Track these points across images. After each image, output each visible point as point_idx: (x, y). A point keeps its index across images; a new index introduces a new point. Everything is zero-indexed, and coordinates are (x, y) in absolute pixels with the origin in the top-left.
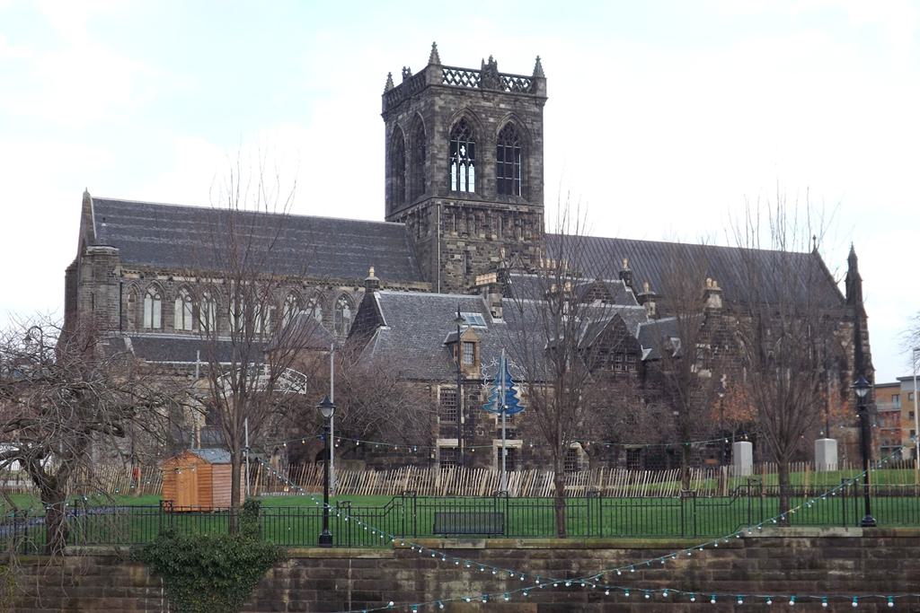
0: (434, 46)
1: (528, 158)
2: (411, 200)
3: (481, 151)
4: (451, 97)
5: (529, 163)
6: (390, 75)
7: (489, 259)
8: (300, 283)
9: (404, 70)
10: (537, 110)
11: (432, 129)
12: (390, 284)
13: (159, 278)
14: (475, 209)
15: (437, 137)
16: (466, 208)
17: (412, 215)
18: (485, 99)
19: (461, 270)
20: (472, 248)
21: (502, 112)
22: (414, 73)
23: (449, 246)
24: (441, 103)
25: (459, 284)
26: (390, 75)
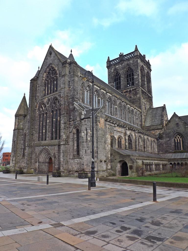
0: (136, 46)
2: (125, 88)
4: (140, 61)
6: (109, 57)
8: (121, 100)
9: (121, 53)
10: (150, 72)
13: (90, 83)
14: (145, 93)
15: (139, 70)
17: (127, 92)
18: (144, 65)
19: (145, 109)
20: (145, 103)
22: (124, 55)
23: (143, 101)
26: (109, 57)
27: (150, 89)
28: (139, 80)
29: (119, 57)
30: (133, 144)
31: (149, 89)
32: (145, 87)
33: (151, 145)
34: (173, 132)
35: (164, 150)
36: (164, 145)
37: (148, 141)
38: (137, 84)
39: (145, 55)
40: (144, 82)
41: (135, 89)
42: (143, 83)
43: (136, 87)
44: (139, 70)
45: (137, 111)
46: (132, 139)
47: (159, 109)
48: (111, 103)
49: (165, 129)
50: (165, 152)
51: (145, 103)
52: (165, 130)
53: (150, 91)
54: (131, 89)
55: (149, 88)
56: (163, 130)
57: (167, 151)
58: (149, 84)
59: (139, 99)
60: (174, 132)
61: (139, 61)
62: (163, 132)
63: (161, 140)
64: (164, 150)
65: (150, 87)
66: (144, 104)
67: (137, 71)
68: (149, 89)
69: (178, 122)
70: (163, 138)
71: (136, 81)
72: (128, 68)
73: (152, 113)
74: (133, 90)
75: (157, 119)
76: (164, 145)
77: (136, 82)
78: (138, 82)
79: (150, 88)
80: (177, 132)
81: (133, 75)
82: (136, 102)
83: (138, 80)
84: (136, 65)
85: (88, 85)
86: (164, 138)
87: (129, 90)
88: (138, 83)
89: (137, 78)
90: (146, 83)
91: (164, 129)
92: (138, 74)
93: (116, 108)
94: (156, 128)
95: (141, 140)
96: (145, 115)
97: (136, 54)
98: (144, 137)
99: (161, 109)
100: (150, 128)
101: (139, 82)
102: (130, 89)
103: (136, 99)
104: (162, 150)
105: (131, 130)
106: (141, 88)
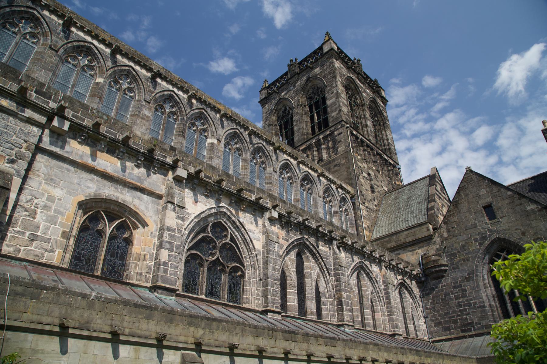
1: (385, 131)
3: (363, 110)
4: (342, 66)
5: (386, 134)
7: (382, 187)
11: (335, 77)
12: (326, 173)
13: (46, 13)
14: (368, 146)
16: (362, 142)
19: (369, 189)
21: (367, 94)
22: (299, 61)
23: (358, 163)
24: (338, 65)
25: (370, 198)
27: (388, 145)
28: (339, 106)
29: (286, 69)
30: (249, 273)
31: (384, 145)
32: (368, 134)
33: (388, 298)
34: (476, 240)
35: (455, 322)
36: (451, 299)
37: (370, 279)
38: (337, 118)
39: (359, 61)
40: (363, 121)
41: (332, 133)
42: (361, 123)
43: (333, 128)
44: (339, 83)
45: (334, 187)
46: (242, 246)
47: (419, 184)
48: (182, 119)
49: (445, 235)
50: (463, 331)
51: (369, 174)
52: (446, 239)
53: (390, 149)
54: (321, 137)
55: (386, 142)
56: (437, 239)
57: (469, 324)
58: (384, 132)
59: (347, 155)
60: (484, 238)
61: (337, 64)
62: (438, 246)
63: (434, 282)
64: (455, 322)
65: (387, 139)
66: (365, 175)
67: (334, 85)
68: (386, 143)
69: (489, 199)
70: (441, 274)
71: (333, 112)
72: (311, 88)
73: (398, 201)
74: (325, 138)
75: (412, 212)
76: (451, 299)
77: (334, 114)
78: (337, 112)
79: (388, 143)
80: (495, 235)
81: (324, 100)
82: (336, 168)
83: (337, 106)
84: (330, 73)
85: (34, 15)
86: (445, 271)
87: (314, 141)
88: (337, 114)
89: (334, 103)
90: (369, 123)
91: (441, 236)
92: (335, 92)
93: (212, 144)
94: (410, 239)
95: (321, 269)
96: (371, 207)
97: (326, 49)
98: (335, 253)
99: (427, 181)
100: (389, 242)
101: (340, 110)
102: (317, 137)
103: (334, 160)
104: (446, 322)
105: (229, 194)
106: (347, 128)
